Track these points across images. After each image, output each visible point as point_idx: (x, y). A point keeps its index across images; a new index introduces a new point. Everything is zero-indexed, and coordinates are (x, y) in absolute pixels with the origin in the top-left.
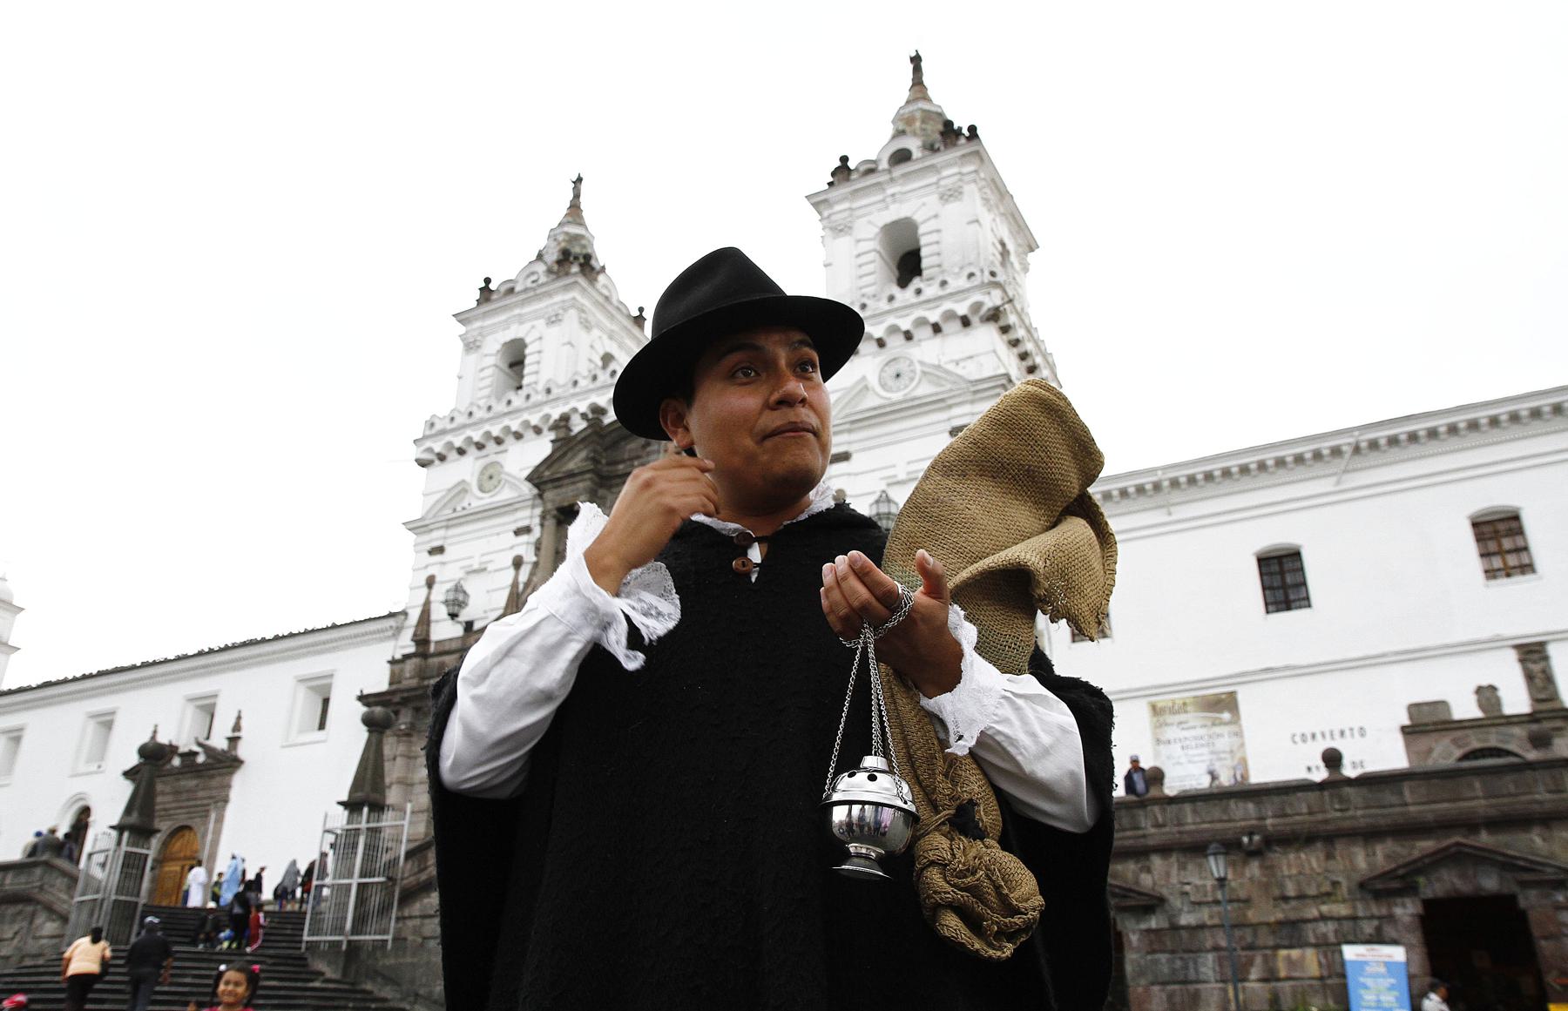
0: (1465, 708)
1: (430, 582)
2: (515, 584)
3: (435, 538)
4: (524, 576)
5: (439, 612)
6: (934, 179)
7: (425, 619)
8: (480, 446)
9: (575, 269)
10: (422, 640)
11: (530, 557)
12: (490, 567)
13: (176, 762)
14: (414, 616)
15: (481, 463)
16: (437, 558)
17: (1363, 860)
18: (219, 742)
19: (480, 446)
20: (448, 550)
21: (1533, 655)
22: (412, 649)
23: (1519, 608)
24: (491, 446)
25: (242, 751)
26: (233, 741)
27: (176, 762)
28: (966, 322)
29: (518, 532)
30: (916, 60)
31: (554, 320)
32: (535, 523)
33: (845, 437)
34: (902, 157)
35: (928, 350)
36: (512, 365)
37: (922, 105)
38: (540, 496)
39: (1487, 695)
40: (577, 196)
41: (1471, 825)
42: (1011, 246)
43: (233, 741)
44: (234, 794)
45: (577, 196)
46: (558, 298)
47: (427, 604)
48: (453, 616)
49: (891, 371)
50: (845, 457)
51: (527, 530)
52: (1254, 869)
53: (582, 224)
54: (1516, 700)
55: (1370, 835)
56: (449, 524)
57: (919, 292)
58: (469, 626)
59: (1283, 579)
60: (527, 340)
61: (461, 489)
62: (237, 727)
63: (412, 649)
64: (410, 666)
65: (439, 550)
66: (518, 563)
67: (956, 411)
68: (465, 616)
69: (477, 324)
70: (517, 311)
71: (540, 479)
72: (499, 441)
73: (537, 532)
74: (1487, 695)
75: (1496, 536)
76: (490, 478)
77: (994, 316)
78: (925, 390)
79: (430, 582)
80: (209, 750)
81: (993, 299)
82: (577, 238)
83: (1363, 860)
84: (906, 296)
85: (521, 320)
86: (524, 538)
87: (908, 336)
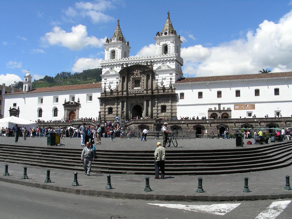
0: (213, 109)
2: (117, 85)
3: (105, 78)
4: (118, 84)
5: (107, 87)
7: (105, 88)
10: (105, 91)
11: (119, 81)
12: (113, 82)
14: (103, 88)
16: (106, 80)
18: (76, 101)
20: (107, 79)
25: (80, 103)
26: (79, 101)
29: (117, 78)
30: (169, 14)
35: (168, 64)
36: (112, 52)
39: (215, 108)
42: (179, 46)
43: (79, 101)
48: (110, 89)
55: (194, 124)
56: (107, 76)
57: (167, 55)
58: (111, 89)
60: (115, 50)
62: (79, 99)
64: (104, 94)
65: (106, 79)
66: (117, 83)
68: (111, 88)
73: (119, 78)
74: (215, 108)
80: (75, 103)
84: (165, 56)
86: (118, 79)
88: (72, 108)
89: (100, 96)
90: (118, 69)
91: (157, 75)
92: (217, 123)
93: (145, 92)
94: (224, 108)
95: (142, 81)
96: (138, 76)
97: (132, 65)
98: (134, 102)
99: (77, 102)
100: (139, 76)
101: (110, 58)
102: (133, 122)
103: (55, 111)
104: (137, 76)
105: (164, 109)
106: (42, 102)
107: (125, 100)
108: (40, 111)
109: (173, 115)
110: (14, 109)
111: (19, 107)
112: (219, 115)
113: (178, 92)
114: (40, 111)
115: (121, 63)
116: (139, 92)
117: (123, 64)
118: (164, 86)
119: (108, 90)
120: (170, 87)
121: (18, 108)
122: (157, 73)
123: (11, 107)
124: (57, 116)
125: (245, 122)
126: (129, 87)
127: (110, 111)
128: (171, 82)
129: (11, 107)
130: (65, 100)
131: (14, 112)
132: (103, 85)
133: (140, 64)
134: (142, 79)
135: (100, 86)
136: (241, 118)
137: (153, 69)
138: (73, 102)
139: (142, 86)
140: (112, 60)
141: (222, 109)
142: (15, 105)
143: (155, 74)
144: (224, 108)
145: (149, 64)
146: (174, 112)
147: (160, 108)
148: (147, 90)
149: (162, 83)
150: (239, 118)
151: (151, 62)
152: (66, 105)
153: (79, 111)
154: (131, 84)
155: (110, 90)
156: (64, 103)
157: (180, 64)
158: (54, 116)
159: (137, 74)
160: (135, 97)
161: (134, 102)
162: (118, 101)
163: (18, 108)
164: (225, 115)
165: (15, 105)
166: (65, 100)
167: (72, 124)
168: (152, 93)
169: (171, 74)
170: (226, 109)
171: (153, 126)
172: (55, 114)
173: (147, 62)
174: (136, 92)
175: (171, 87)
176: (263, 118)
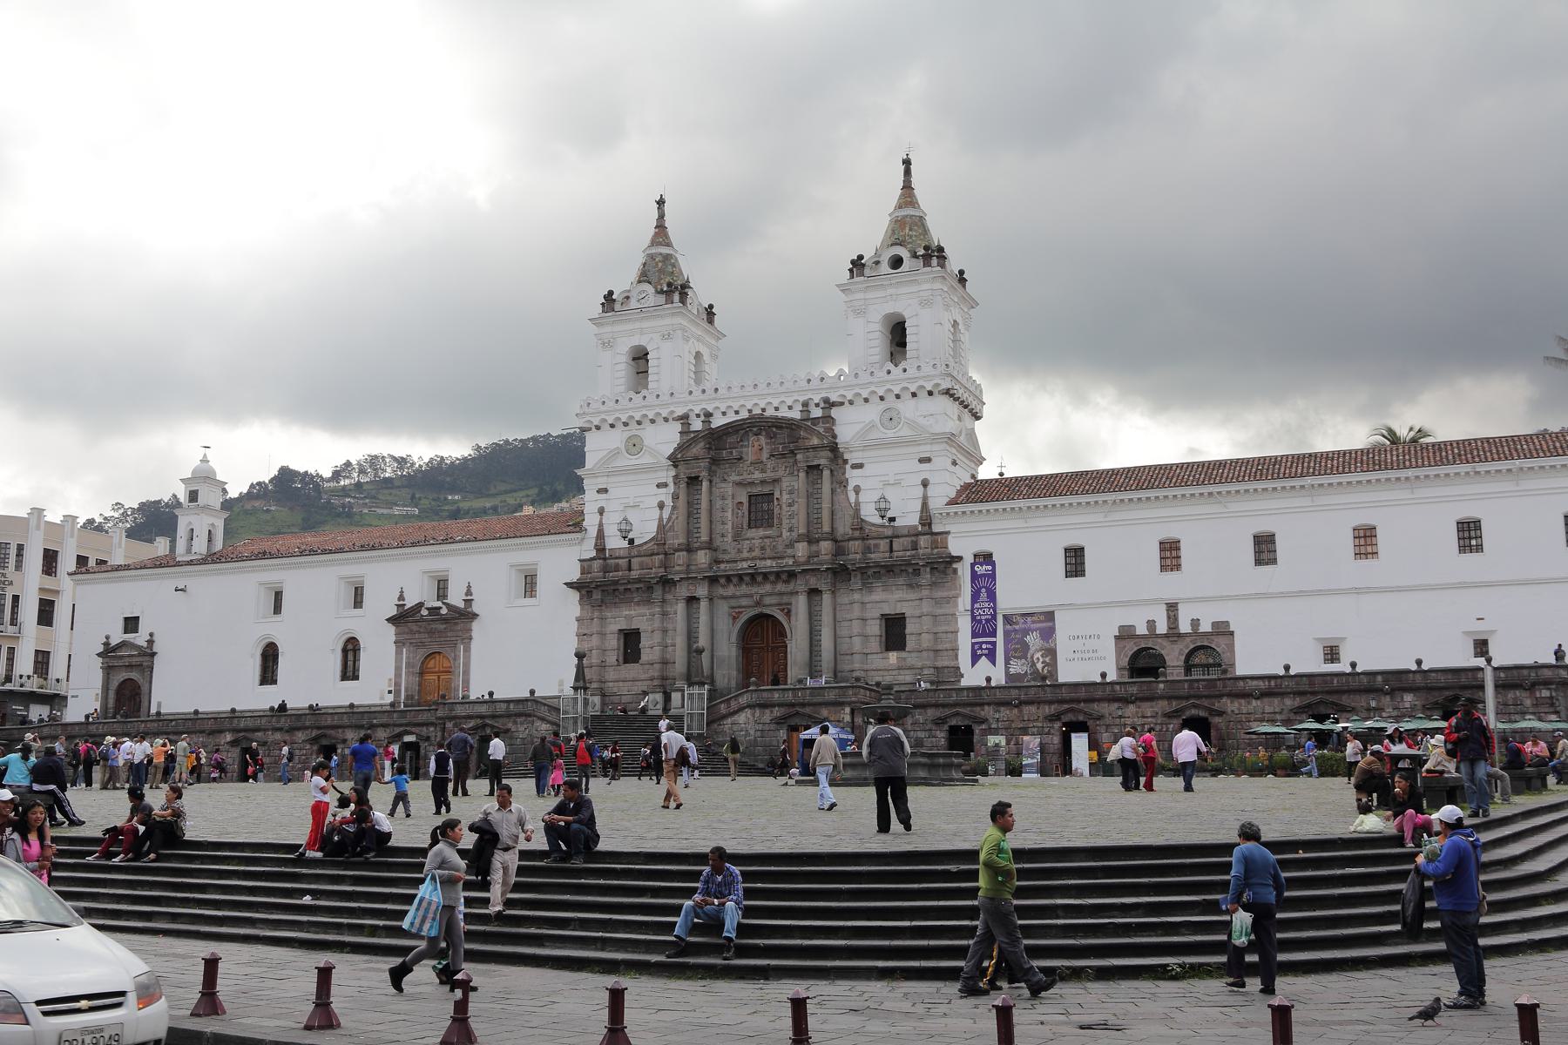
0: (1142, 630)
1: (601, 511)
2: (661, 519)
4: (666, 515)
6: (914, 289)
7: (601, 535)
8: (626, 424)
9: (676, 297)
10: (600, 549)
11: (669, 503)
13: (425, 612)
14: (593, 532)
15: (626, 435)
16: (604, 496)
17: (1048, 710)
18: (456, 598)
19: (626, 424)
21: (1172, 608)
22: (593, 554)
23: (1171, 586)
24: (633, 425)
25: (475, 608)
26: (468, 602)
27: (425, 612)
28: (930, 393)
30: (907, 162)
31: (667, 337)
32: (670, 481)
33: (860, 454)
34: (897, 262)
35: (907, 408)
37: (909, 211)
38: (676, 466)
39: (1151, 624)
40: (661, 216)
41: (1078, 701)
43: (468, 602)
44: (474, 634)
45: (661, 216)
46: (668, 321)
47: (601, 525)
49: (888, 416)
50: (860, 466)
51: (665, 485)
52: (1016, 711)
53: (669, 245)
54: (1162, 628)
55: (1050, 702)
58: (631, 541)
59: (1075, 561)
61: (615, 453)
62: (469, 592)
63: (593, 554)
64: (597, 564)
65: (605, 491)
66: (661, 506)
67: (922, 448)
69: (608, 329)
70: (637, 325)
71: (674, 460)
72: (639, 423)
73: (671, 488)
74: (1151, 624)
75: (1171, 549)
76: (634, 446)
77: (948, 392)
78: (905, 432)
79: (601, 511)
81: (946, 385)
82: (667, 257)
83: (1048, 710)
85: (642, 332)
87: (898, 397)
88: (435, 629)
89: (575, 575)
90: (666, 439)
91: (855, 466)
92: (1169, 698)
93: (801, 550)
94: (1195, 623)
95: (785, 496)
96: (763, 471)
97: (731, 418)
98: (744, 602)
99: (461, 605)
100: (769, 475)
101: (622, 388)
102: (743, 700)
103: (351, 649)
104: (758, 475)
105: (894, 632)
106: (277, 609)
107: (702, 591)
108: (270, 656)
109: (939, 664)
110: (123, 644)
111: (151, 635)
112: (1174, 657)
113: (963, 542)
114: (270, 656)
115: (680, 412)
116: (768, 552)
117: (684, 419)
118: (892, 519)
119: (615, 542)
120: (923, 525)
121: (151, 642)
122: (853, 458)
123: (107, 637)
124: (356, 678)
125: (1313, 693)
126: (718, 528)
127: (631, 642)
128: (925, 505)
129: (107, 637)
130: (401, 598)
131: (126, 661)
132: (591, 522)
133: (770, 412)
134: (785, 483)
135: (575, 524)
136: (1292, 672)
137: (835, 437)
138: (439, 604)
139: (785, 521)
140: (632, 394)
141: (1184, 627)
142: (131, 624)
143: (846, 462)
144: (1195, 623)
145: (817, 413)
146: (948, 646)
147: (875, 628)
148: (811, 540)
149: (883, 505)
150: (1282, 672)
151: (829, 404)
152: (403, 618)
153: (474, 645)
154: (729, 514)
155: (625, 544)
156: (394, 612)
157: (971, 411)
158: (344, 677)
159: (758, 463)
160: (754, 577)
161: (749, 598)
162: (664, 601)
163: (151, 642)
164: (1199, 658)
165: (131, 624)
166: (401, 598)
167: (440, 713)
168: (839, 551)
169: (928, 460)
170: (1205, 627)
171: (848, 718)
172: (349, 672)
173: (805, 404)
174: (757, 553)
175: (926, 520)
176: (1409, 672)
